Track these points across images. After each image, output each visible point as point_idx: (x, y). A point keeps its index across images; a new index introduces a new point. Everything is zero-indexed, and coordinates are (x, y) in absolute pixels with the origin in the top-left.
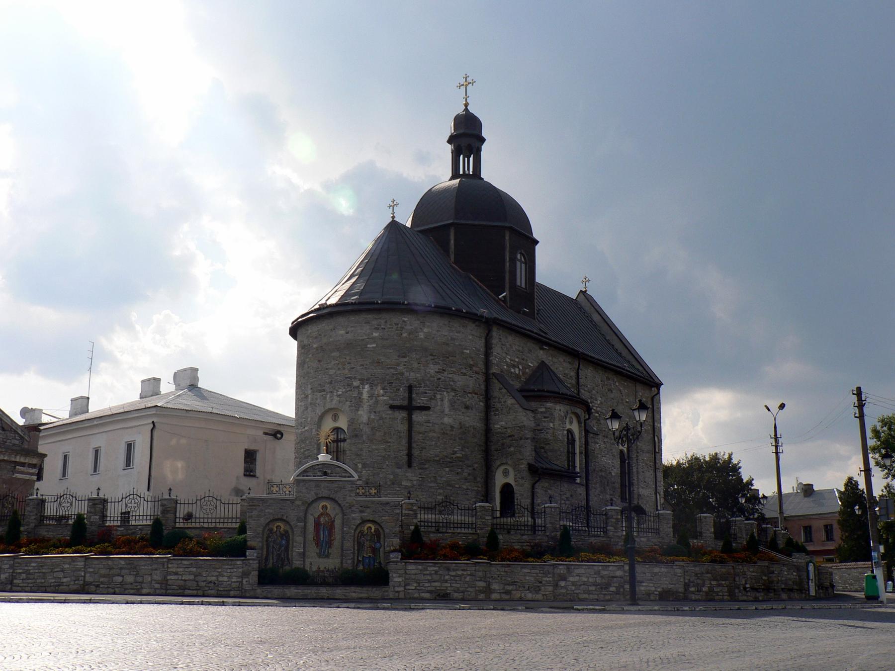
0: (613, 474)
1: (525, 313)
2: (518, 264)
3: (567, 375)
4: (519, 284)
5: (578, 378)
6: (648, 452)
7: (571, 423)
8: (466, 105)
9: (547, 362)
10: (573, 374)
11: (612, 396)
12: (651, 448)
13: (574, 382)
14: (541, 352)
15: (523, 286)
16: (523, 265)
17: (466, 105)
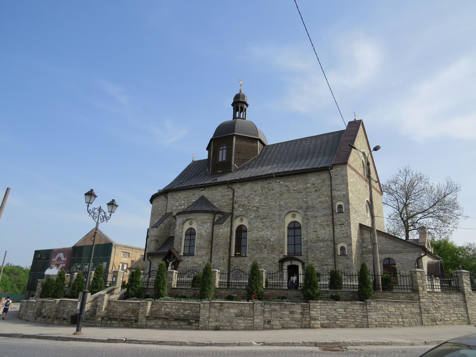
0: (272, 240)
1: (219, 173)
2: (221, 152)
3: (225, 195)
4: (220, 160)
5: (233, 194)
6: (325, 215)
7: (191, 224)
8: (240, 91)
9: (206, 196)
10: (230, 193)
11: (274, 192)
12: (329, 212)
13: (231, 197)
14: (203, 192)
15: (224, 159)
16: (225, 151)
17: (240, 91)
